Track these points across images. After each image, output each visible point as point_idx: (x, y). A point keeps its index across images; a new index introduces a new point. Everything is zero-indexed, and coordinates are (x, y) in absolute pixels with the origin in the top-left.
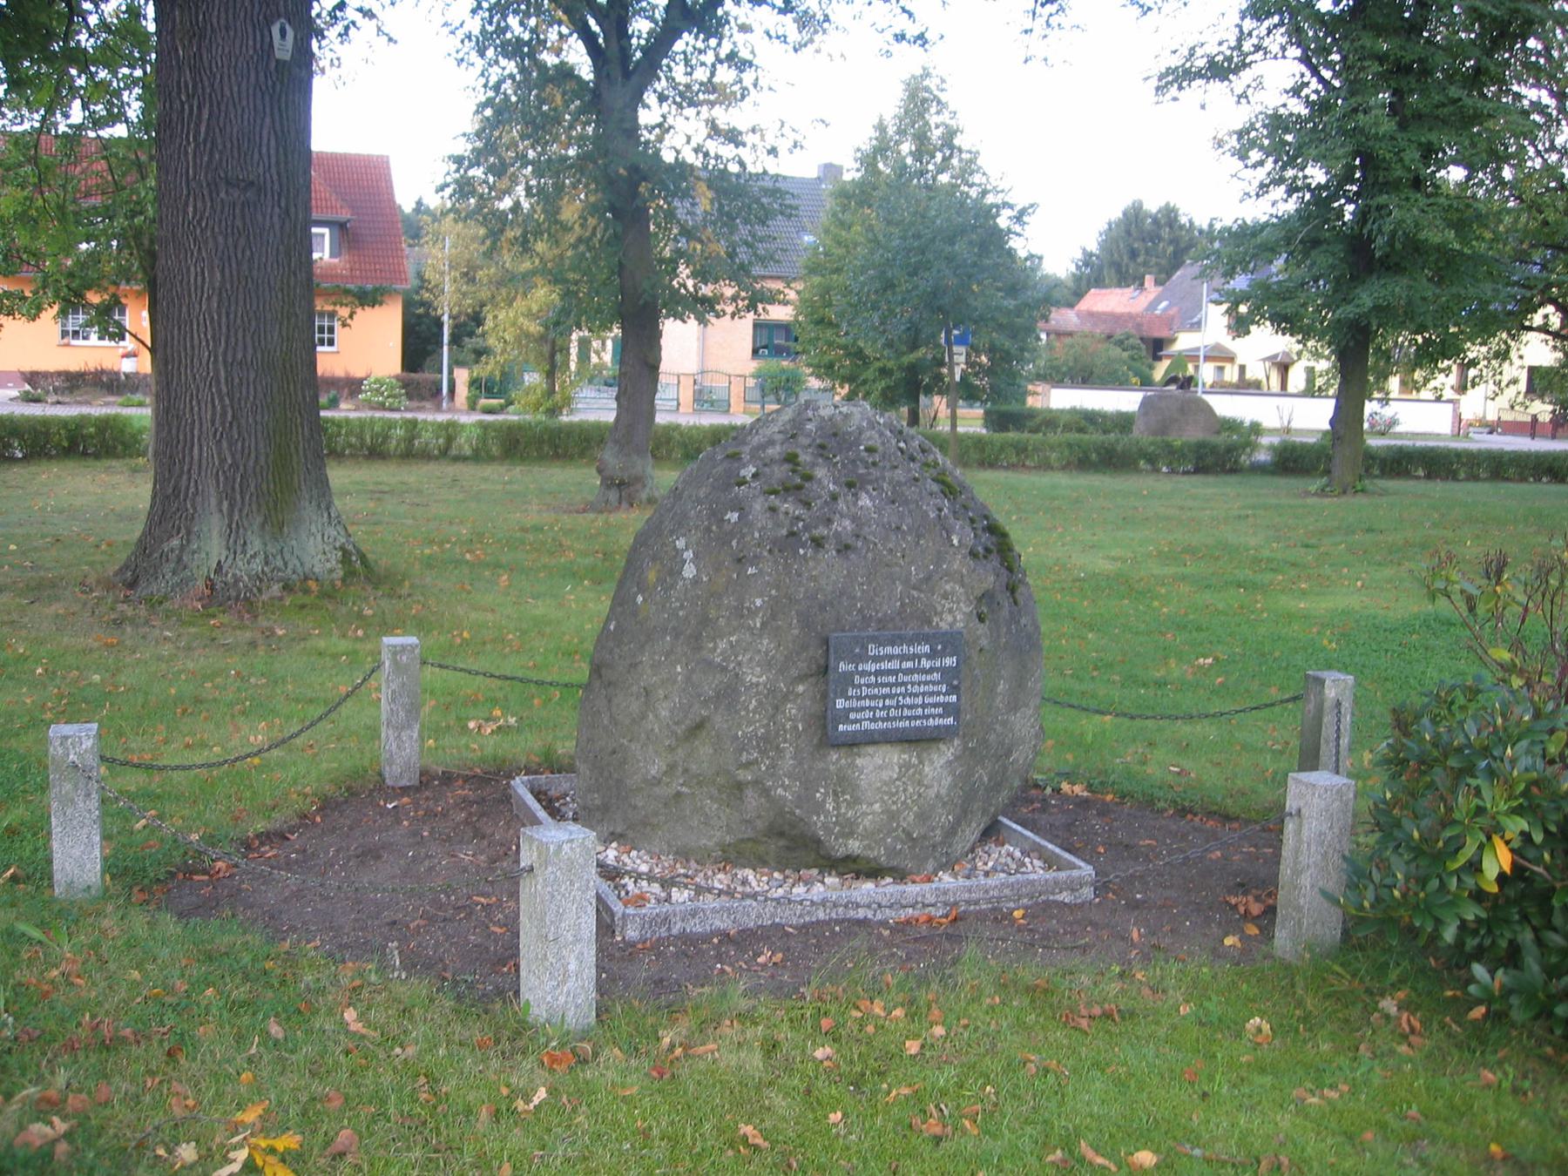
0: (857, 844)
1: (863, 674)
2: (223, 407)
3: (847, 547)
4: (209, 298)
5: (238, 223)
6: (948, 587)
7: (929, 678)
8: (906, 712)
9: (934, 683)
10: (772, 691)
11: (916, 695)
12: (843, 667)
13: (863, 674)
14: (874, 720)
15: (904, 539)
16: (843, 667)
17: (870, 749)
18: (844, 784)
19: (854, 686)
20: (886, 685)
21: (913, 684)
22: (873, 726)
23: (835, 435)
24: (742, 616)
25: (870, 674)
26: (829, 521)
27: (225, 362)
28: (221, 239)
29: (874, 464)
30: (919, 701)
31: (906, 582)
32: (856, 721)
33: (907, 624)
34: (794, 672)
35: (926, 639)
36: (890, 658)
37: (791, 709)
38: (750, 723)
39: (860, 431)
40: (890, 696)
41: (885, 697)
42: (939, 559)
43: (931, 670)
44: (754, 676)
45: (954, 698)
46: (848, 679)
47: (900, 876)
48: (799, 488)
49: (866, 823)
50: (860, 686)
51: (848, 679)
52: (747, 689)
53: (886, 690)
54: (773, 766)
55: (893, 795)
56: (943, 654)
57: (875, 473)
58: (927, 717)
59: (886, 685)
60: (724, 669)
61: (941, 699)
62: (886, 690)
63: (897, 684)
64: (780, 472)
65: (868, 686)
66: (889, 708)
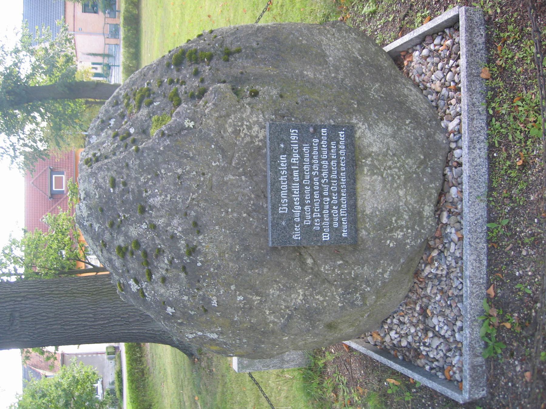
0: (426, 208)
1: (303, 217)
2: (114, 321)
3: (195, 224)
4: (65, 330)
5: (30, 319)
6: (230, 130)
8: (334, 176)
9: (311, 150)
10: (311, 285)
11: (321, 167)
12: (296, 236)
13: (303, 217)
14: (339, 205)
15: (189, 172)
16: (296, 236)
17: (360, 202)
18: (384, 225)
19: (312, 225)
20: (312, 195)
21: (312, 170)
22: (344, 206)
23: (102, 210)
24: (251, 308)
25: (303, 210)
26: (173, 237)
27: (94, 322)
28: (38, 327)
29: (125, 184)
31: (225, 170)
32: (340, 222)
34: (298, 270)
35: (275, 159)
36: (290, 191)
37: (324, 268)
38: (333, 298)
39: (98, 186)
41: (322, 196)
42: (205, 139)
43: (301, 153)
44: (298, 297)
45: (323, 131)
46: (307, 230)
48: (146, 254)
49: (412, 201)
50: (312, 219)
51: (307, 230)
52: (307, 302)
53: (316, 196)
54: (367, 282)
55: (393, 178)
56: (288, 142)
57: (132, 185)
58: (338, 156)
59: (312, 195)
60: (290, 317)
62: (316, 196)
63: (312, 185)
64: (133, 265)
65: (312, 212)
66: (330, 191)
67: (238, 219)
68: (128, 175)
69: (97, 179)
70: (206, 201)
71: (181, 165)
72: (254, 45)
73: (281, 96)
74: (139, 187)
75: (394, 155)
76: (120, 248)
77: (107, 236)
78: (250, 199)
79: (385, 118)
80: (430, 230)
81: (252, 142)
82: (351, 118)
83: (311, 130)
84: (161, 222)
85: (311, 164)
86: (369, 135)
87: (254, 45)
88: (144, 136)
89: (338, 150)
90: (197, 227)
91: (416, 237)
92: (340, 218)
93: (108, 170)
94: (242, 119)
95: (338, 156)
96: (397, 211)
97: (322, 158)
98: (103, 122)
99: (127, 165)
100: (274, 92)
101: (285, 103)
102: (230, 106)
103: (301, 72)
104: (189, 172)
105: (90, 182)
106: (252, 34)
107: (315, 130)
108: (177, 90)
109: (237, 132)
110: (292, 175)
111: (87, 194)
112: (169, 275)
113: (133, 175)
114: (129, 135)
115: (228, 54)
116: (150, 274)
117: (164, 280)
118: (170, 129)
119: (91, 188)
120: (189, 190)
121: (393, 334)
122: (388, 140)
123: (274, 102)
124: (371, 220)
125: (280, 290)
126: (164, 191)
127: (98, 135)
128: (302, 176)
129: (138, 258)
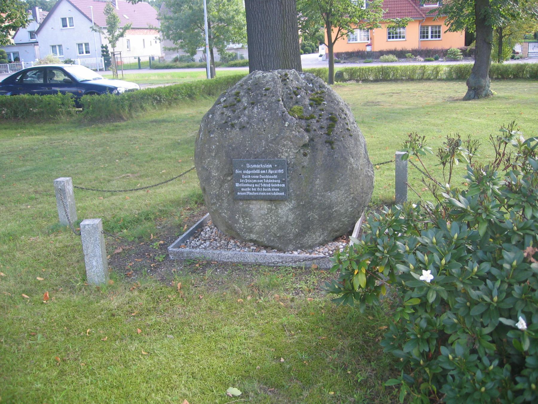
0: (254, 236)
1: (245, 174)
3: (244, 127)
4: (258, 34)
5: (265, 8)
6: (285, 143)
7: (272, 177)
9: (275, 179)
10: (219, 179)
11: (268, 183)
12: (237, 171)
13: (245, 174)
14: (251, 191)
15: (265, 124)
16: (237, 171)
17: (254, 202)
18: (245, 214)
19: (242, 179)
20: (255, 179)
21: (266, 179)
22: (251, 194)
23: (256, 84)
24: (210, 152)
25: (248, 174)
26: (239, 117)
27: (263, 55)
28: (260, 14)
29: (265, 95)
30: (269, 185)
31: (267, 140)
32: (244, 192)
33: (269, 156)
35: (270, 162)
36: (256, 169)
38: (215, 189)
39: (267, 82)
40: (257, 183)
41: (255, 183)
42: (281, 131)
44: (215, 174)
45: (284, 185)
46: (239, 176)
47: (280, 250)
48: (234, 105)
50: (244, 179)
51: (239, 176)
54: (220, 205)
56: (277, 168)
57: (264, 98)
58: (273, 192)
59: (255, 179)
61: (278, 185)
63: (259, 179)
64: (231, 99)
65: (248, 179)
66: (257, 187)
67: (246, 146)
68: (269, 96)
69: (271, 81)
70: (253, 132)
71: (269, 121)
72: (335, 156)
73: (303, 167)
74: (263, 102)
75: (278, 221)
76: (239, 93)
77: (245, 87)
78: (254, 151)
79: (297, 218)
80: (243, 236)
81: (280, 153)
82: (294, 200)
83: (284, 179)
84: (246, 112)
85: (269, 179)
86: (287, 209)
87: (335, 156)
88: (294, 102)
89: (276, 192)
90: (242, 128)
91: (240, 229)
92: (245, 192)
93: (274, 87)
94: (291, 148)
95: (273, 192)
96: (252, 220)
97: (272, 184)
98: (312, 80)
99: (273, 96)
100: (305, 164)
101: (299, 168)
102: (296, 143)
103: (318, 178)
104: (265, 124)
105: (270, 78)
106: (342, 155)
107: (284, 181)
108: (315, 118)
109: (284, 146)
110: (263, 170)
111: (265, 77)
112: (224, 116)
113: (269, 99)
114: (297, 95)
115: (331, 143)
116: (226, 107)
117: (223, 113)
118: (285, 115)
119: (267, 79)
120: (258, 124)
121: (209, 229)
122: (285, 219)
123: (300, 164)
124: (247, 207)
125: (217, 165)
126: (259, 113)
127: (305, 78)
128: (263, 174)
129: (234, 102)
